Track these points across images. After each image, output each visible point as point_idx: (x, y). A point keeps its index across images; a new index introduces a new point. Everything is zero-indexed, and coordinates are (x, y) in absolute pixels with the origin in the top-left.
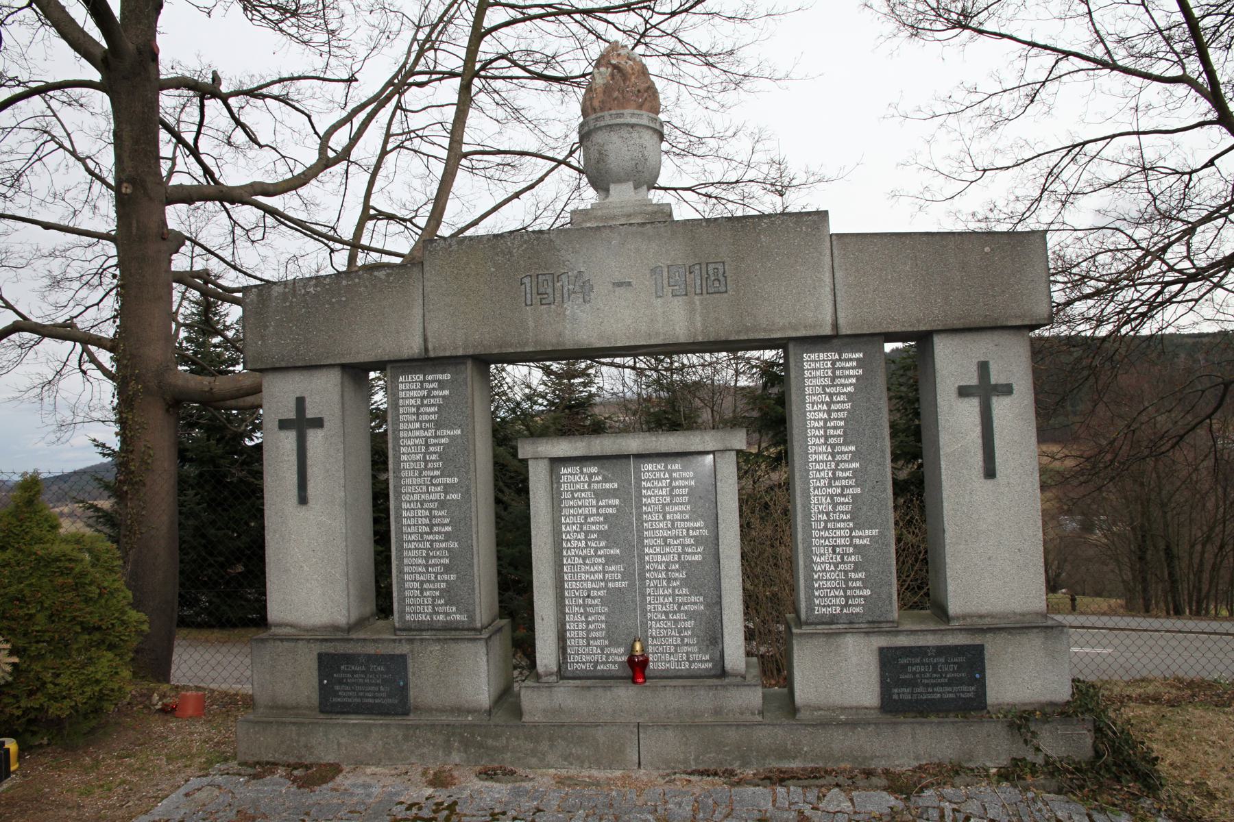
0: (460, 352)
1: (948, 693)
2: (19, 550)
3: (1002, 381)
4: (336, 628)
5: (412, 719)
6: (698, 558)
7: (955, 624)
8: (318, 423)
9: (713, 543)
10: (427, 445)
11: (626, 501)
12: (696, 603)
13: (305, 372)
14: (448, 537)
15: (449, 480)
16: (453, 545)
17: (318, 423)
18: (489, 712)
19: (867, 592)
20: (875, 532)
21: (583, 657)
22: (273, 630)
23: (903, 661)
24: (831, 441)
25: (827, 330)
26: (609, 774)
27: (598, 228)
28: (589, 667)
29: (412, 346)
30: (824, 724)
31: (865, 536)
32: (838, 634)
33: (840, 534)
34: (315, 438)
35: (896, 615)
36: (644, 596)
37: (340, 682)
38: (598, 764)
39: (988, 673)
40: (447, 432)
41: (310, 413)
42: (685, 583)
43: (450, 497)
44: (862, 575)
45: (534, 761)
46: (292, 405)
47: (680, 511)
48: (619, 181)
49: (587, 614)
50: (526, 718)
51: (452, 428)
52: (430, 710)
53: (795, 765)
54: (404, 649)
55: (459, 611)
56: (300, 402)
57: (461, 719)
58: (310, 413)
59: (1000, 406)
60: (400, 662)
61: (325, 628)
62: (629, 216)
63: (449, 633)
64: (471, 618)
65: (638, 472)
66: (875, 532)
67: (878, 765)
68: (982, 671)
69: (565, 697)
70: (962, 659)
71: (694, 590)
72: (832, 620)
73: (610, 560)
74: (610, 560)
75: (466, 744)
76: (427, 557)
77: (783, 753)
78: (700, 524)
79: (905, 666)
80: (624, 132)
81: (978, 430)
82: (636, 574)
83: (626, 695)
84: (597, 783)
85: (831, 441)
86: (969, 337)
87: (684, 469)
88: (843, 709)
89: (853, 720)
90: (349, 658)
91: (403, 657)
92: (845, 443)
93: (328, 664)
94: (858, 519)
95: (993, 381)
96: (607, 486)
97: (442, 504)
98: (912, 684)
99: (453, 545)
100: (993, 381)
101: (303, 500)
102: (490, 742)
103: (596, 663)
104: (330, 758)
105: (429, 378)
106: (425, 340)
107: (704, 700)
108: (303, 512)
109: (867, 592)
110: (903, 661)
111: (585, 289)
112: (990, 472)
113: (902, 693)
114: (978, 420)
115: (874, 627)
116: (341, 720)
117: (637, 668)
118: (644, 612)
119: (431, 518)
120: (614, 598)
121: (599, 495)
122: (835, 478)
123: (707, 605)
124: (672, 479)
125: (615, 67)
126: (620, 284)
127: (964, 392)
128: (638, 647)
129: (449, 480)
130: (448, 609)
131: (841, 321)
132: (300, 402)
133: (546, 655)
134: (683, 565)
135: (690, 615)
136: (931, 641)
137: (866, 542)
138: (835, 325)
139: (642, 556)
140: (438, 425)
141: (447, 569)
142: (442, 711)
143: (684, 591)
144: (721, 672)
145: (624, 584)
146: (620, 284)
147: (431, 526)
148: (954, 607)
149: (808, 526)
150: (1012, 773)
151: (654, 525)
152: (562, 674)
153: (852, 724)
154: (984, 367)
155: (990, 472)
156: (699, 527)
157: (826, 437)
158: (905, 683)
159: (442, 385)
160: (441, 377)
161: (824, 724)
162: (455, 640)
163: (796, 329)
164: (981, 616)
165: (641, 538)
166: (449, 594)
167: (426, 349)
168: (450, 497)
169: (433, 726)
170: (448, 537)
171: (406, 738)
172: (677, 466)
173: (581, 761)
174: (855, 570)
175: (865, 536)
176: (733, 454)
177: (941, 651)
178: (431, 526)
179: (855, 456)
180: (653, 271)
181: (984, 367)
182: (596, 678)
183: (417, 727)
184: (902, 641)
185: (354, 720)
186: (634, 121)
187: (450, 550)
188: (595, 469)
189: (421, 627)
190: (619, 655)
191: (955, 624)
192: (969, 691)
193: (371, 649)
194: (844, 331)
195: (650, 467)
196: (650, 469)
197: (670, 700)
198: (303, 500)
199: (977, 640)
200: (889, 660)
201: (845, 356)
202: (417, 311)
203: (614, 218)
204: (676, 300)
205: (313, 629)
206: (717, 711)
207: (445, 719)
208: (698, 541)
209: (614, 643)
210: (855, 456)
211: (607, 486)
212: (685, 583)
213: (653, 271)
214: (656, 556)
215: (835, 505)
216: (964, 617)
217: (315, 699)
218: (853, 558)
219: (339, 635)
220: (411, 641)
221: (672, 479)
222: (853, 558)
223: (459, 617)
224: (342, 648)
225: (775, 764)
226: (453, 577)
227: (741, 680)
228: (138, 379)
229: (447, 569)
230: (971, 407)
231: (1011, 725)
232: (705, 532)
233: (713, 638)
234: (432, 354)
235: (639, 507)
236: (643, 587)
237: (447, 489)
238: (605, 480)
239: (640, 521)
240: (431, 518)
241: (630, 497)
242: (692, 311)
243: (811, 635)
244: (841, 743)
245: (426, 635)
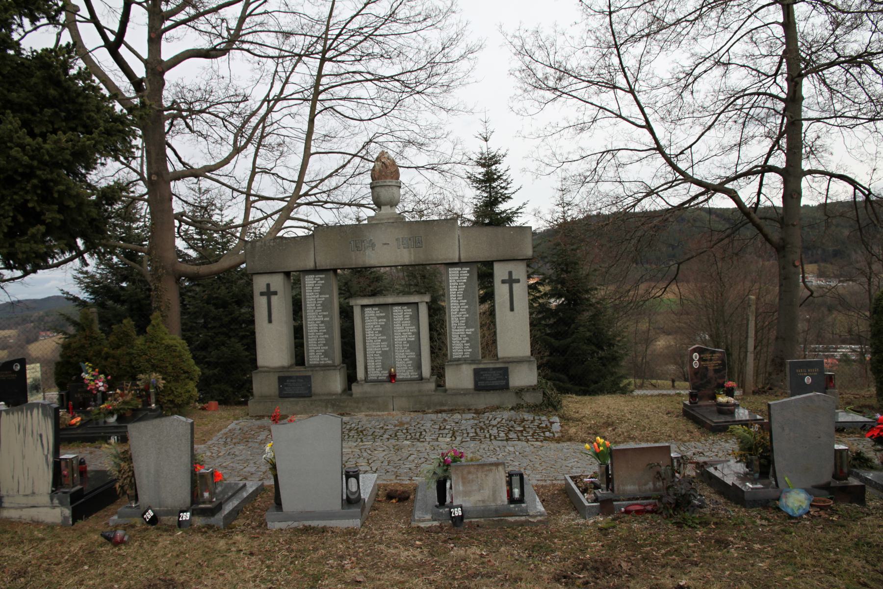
0: (328, 268)
1: (497, 383)
2: (157, 343)
3: (517, 278)
4: (283, 367)
5: (313, 398)
6: (413, 339)
7: (500, 360)
8: (275, 293)
9: (418, 334)
10: (316, 301)
11: (388, 319)
12: (413, 355)
13: (270, 275)
14: (325, 334)
15: (325, 313)
16: (326, 336)
17: (275, 293)
18: (341, 394)
19: (470, 350)
20: (473, 330)
21: (373, 375)
22: (260, 369)
23: (482, 373)
24: (458, 298)
25: (457, 261)
26: (383, 413)
27: (377, 224)
28: (376, 378)
29: (310, 265)
30: (455, 394)
31: (470, 331)
32: (460, 364)
33: (461, 330)
34: (274, 299)
35: (480, 358)
36: (394, 353)
37: (286, 386)
38: (379, 410)
39: (510, 376)
40: (324, 296)
41: (272, 289)
42: (409, 348)
43: (326, 319)
44: (468, 344)
45: (357, 410)
46: (265, 286)
47: (407, 322)
48: (385, 205)
49: (375, 360)
50: (354, 396)
51: (325, 294)
52: (319, 395)
53: (445, 408)
54: (310, 373)
55: (329, 360)
56: (268, 285)
57: (330, 398)
58: (272, 289)
59: (515, 286)
60: (309, 377)
61: (279, 368)
62: (388, 219)
63: (325, 367)
64: (334, 362)
65: (392, 310)
66: (473, 330)
67: (473, 407)
68: (508, 376)
69: (367, 388)
70: (501, 372)
71: (412, 350)
72: (459, 360)
73: (382, 340)
74: (382, 340)
75: (333, 405)
76: (317, 341)
77: (442, 404)
78: (414, 327)
79: (482, 375)
80: (386, 188)
81: (508, 294)
82: (392, 345)
83: (388, 386)
84: (379, 416)
85: (458, 298)
86: (506, 262)
87: (408, 308)
88: (462, 389)
89: (465, 392)
90: (290, 377)
91: (309, 377)
92: (463, 299)
93: (282, 380)
94: (468, 326)
95: (514, 278)
96: (381, 314)
97: (322, 322)
98: (485, 380)
99: (326, 336)
100: (514, 278)
101: (270, 321)
102: (341, 404)
103: (378, 377)
104: (283, 413)
105: (317, 276)
106: (315, 263)
107: (415, 387)
108: (270, 325)
109: (470, 350)
110: (482, 373)
111: (373, 246)
112: (512, 309)
113: (481, 384)
114: (508, 291)
115: (473, 361)
116: (287, 399)
117: (392, 377)
118: (395, 358)
119: (318, 327)
120: (384, 354)
121: (379, 318)
122: (460, 311)
123: (417, 355)
124: (404, 312)
125: (383, 163)
126: (385, 244)
127: (503, 282)
128: (393, 370)
129: (325, 313)
130: (325, 359)
131: (462, 257)
132: (268, 285)
133: (360, 374)
134: (408, 342)
135: (411, 359)
136: (491, 366)
137: (470, 333)
138: (460, 258)
139: (393, 339)
140: (320, 294)
141: (325, 345)
142: (324, 395)
143: (408, 351)
144: (421, 378)
145: (387, 349)
146: (385, 244)
147: (319, 330)
148: (500, 355)
149: (451, 328)
150: (517, 408)
151: (398, 328)
152: (366, 380)
153: (465, 394)
154: (510, 273)
155: (512, 309)
156: (414, 329)
157: (457, 297)
158: (482, 380)
159: (321, 279)
160: (321, 276)
161: (455, 394)
162: (328, 370)
163: (446, 260)
164: (509, 358)
165: (393, 333)
166: (326, 354)
167: (316, 266)
168: (326, 319)
169: (321, 400)
170: (325, 334)
171: (311, 404)
172: (406, 307)
173: (373, 410)
174: (467, 343)
175: (470, 331)
176: (425, 304)
177: (494, 369)
178: (319, 330)
179: (467, 304)
180: (397, 240)
181: (510, 273)
182: (378, 381)
183: (315, 400)
184: (482, 366)
185: (292, 399)
186: (390, 184)
187: (325, 338)
188: (377, 309)
189: (315, 366)
190: (386, 373)
191: (500, 360)
192: (503, 383)
193: (298, 374)
194: (463, 260)
195: (396, 308)
196: (396, 309)
197: (403, 388)
198: (270, 321)
199: (506, 365)
200: (477, 372)
201: (464, 269)
202: (312, 253)
203: (383, 219)
204: (405, 250)
205: (275, 368)
206: (420, 391)
207: (325, 397)
208: (413, 333)
209: (384, 369)
210: (467, 304)
211: (381, 314)
212: (409, 348)
213: (397, 240)
214: (398, 338)
215: (460, 320)
216: (503, 358)
217: (277, 393)
218: (466, 339)
219: (285, 370)
220: (312, 371)
221: (404, 312)
222: (466, 339)
223: (329, 362)
224: (286, 374)
225: (438, 408)
226: (327, 348)
227: (428, 380)
228: (163, 267)
229: (325, 345)
230: (506, 286)
231: (517, 393)
232: (415, 330)
233: (419, 367)
234: (318, 268)
235: (393, 322)
236: (394, 349)
237: (324, 316)
238: (381, 312)
239: (393, 327)
240: (318, 327)
241: (389, 318)
242: (411, 254)
243: (451, 365)
244: (461, 400)
245: (317, 369)
